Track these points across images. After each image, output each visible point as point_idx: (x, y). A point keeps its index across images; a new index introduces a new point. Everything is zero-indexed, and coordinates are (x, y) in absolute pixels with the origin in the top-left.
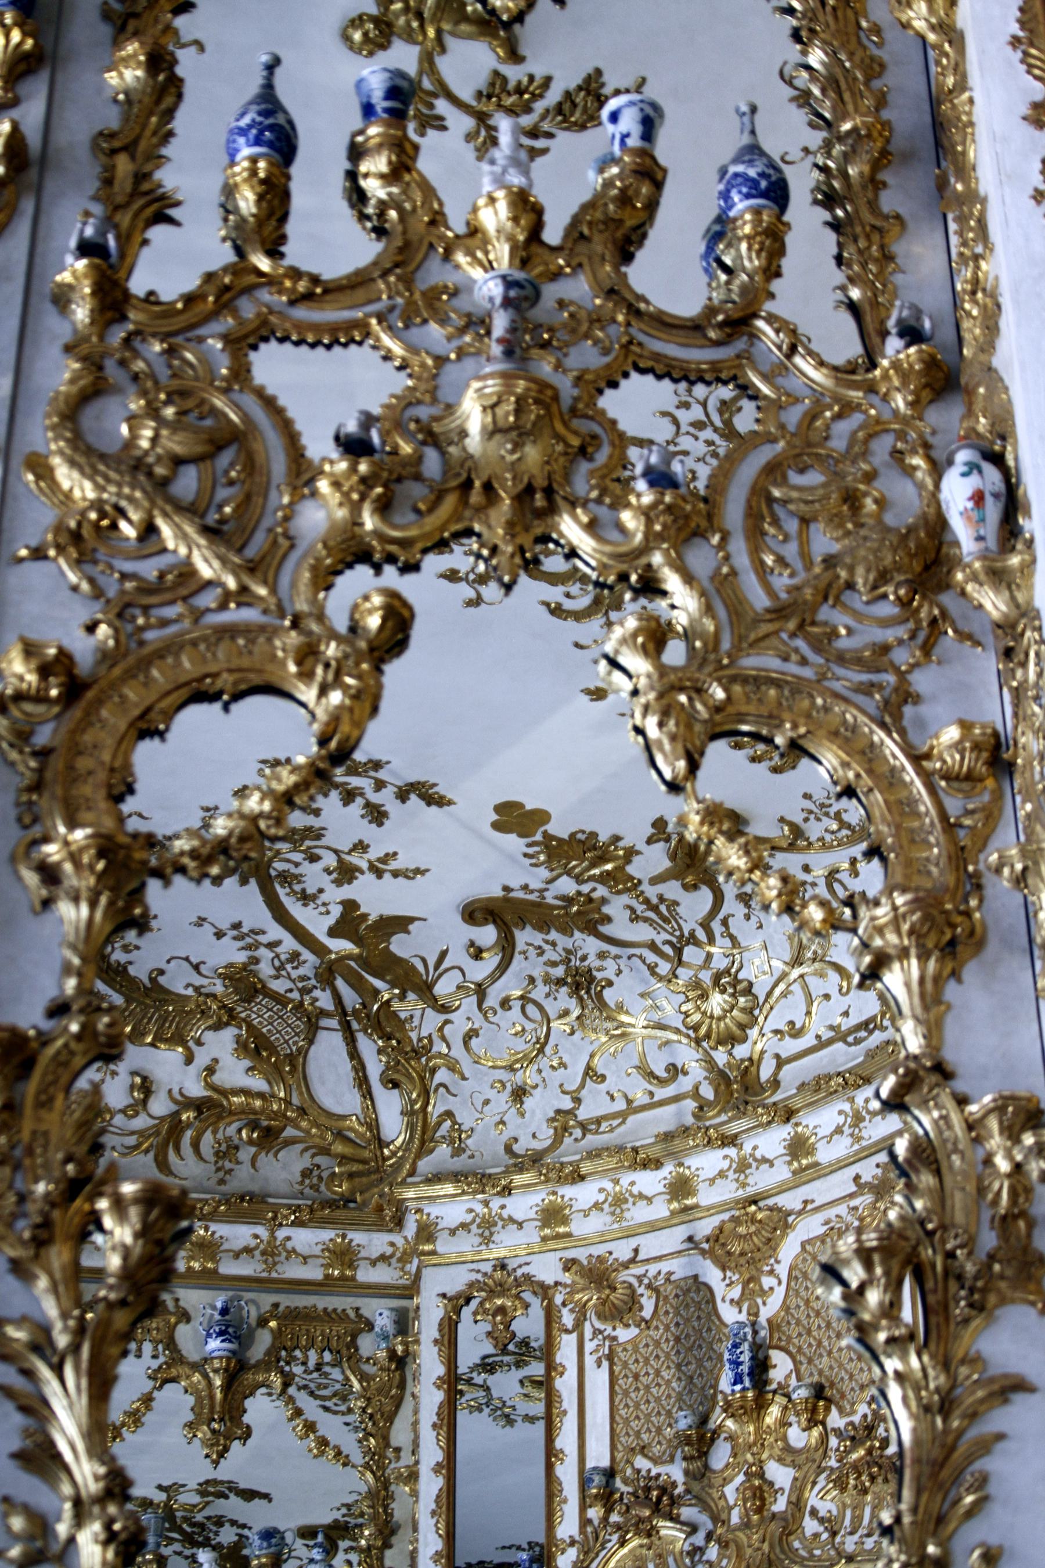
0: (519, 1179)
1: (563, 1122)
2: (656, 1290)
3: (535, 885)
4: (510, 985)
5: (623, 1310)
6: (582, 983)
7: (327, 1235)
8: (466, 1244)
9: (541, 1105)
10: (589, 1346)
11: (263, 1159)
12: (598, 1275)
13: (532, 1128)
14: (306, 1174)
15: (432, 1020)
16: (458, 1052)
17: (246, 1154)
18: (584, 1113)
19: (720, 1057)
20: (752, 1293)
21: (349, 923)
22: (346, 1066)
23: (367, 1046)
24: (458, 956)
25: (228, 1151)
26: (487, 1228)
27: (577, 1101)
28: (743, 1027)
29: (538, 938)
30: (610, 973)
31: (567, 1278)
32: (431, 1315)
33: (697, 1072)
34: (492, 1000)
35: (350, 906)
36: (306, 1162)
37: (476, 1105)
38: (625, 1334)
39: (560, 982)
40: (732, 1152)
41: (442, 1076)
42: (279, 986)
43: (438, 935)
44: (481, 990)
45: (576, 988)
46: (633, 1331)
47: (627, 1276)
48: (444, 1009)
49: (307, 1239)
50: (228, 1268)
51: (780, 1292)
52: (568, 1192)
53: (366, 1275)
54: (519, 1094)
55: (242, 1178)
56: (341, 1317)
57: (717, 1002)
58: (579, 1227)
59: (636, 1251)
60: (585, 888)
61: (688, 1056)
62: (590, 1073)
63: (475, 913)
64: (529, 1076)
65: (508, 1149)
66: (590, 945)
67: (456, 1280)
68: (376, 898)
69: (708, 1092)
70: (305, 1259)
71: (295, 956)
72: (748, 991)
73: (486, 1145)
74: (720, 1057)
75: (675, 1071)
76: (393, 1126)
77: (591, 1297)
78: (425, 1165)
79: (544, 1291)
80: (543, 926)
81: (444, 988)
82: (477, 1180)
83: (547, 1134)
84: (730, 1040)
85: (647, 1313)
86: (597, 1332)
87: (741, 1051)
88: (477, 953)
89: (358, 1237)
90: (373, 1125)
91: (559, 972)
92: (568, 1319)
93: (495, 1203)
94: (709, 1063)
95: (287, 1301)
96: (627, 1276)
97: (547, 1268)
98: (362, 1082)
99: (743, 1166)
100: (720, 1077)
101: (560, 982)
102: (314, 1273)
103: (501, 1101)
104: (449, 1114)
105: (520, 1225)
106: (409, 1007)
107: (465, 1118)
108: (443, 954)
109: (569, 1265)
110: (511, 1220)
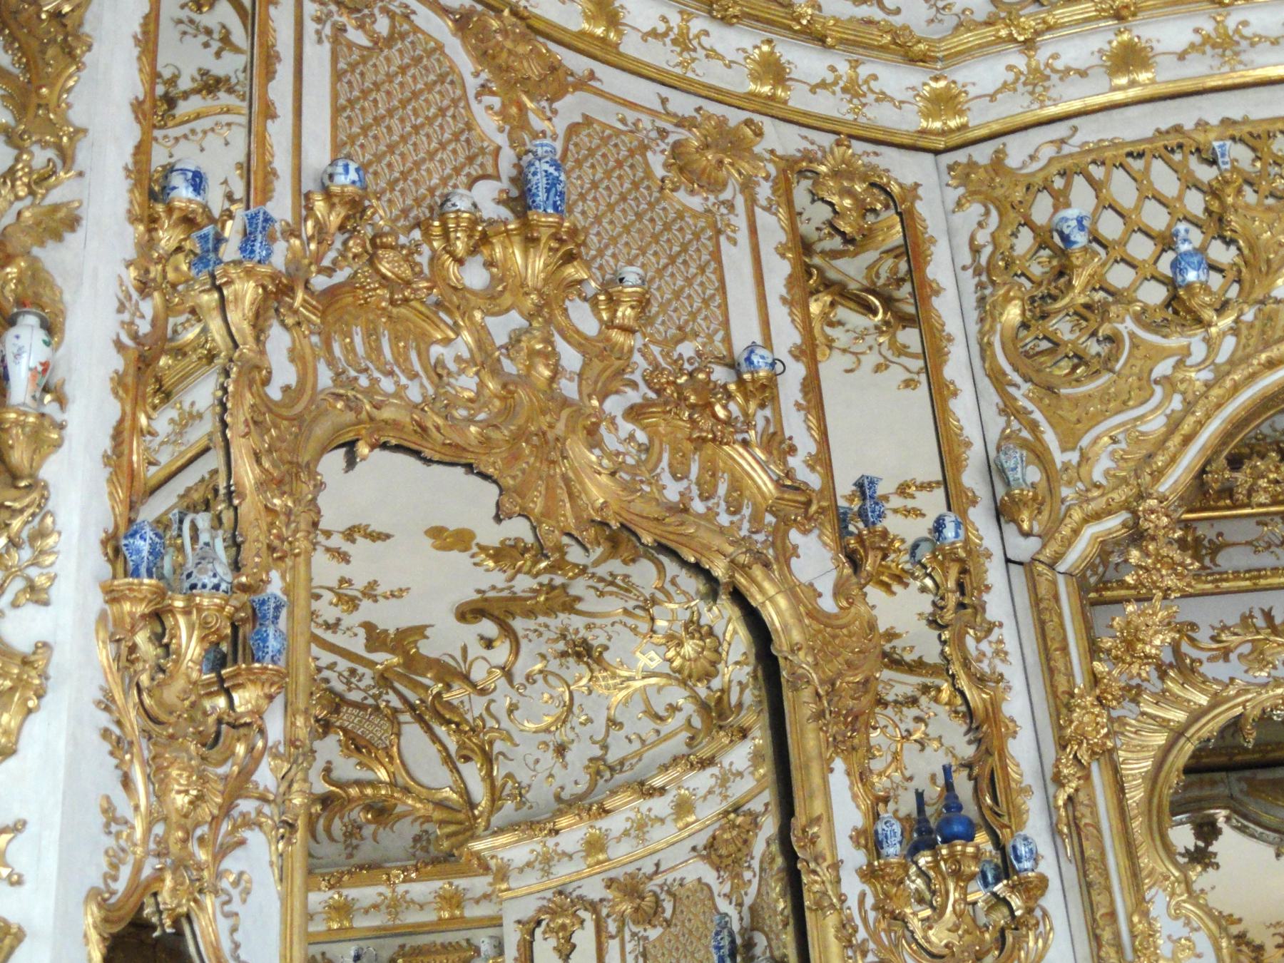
0: (563, 822)
1: (600, 768)
2: (673, 895)
3: (500, 585)
4: (528, 663)
5: (650, 915)
6: (584, 652)
7: (437, 885)
8: (532, 880)
9: (580, 754)
10: (629, 947)
11: (383, 833)
12: (631, 888)
13: (574, 777)
14: (417, 839)
15: (478, 706)
16: (506, 723)
17: (368, 831)
18: (612, 757)
19: (701, 690)
20: (739, 885)
21: (376, 639)
22: (434, 749)
23: (441, 730)
24: (476, 650)
25: (353, 831)
26: (546, 862)
27: (605, 747)
28: (714, 664)
29: (531, 624)
30: (602, 640)
31: (609, 894)
32: (512, 937)
33: (689, 708)
34: (519, 679)
35: (369, 627)
36: (416, 829)
37: (530, 766)
38: (653, 933)
39: (564, 654)
40: (714, 770)
41: (498, 746)
42: (355, 696)
43: (447, 638)
44: (508, 674)
45: (579, 656)
46: (659, 930)
47: (652, 886)
48: (483, 692)
49: (421, 890)
50: (362, 922)
51: (756, 881)
52: (604, 823)
53: (472, 912)
54: (561, 750)
55: (367, 851)
56: (456, 947)
57: (689, 648)
58: (620, 851)
59: (657, 865)
60: (545, 579)
61: (678, 696)
62: (613, 723)
63: (469, 613)
64: (563, 735)
65: (558, 798)
66: (577, 622)
67: (527, 909)
68: (390, 617)
69: (697, 722)
70: (422, 907)
71: (353, 672)
72: (711, 633)
73: (541, 794)
74: (701, 690)
75: (674, 709)
76: (479, 792)
77: (626, 907)
78: (496, 820)
79: (593, 907)
80: (530, 613)
81: (478, 674)
82: (529, 825)
83: (584, 781)
84: (708, 676)
85: (668, 914)
86: (634, 934)
87: (716, 683)
88: (489, 644)
89: (462, 883)
90: (465, 793)
91: (561, 646)
92: (612, 927)
93: (551, 842)
94: (695, 697)
95: (412, 942)
96: (652, 886)
97: (594, 890)
98: (448, 759)
99: (724, 781)
100: (704, 707)
101: (564, 654)
102: (429, 916)
103: (549, 758)
104: (509, 776)
105: (570, 857)
106: (457, 694)
107: (523, 776)
108: (465, 650)
109: (610, 883)
110: (564, 854)
